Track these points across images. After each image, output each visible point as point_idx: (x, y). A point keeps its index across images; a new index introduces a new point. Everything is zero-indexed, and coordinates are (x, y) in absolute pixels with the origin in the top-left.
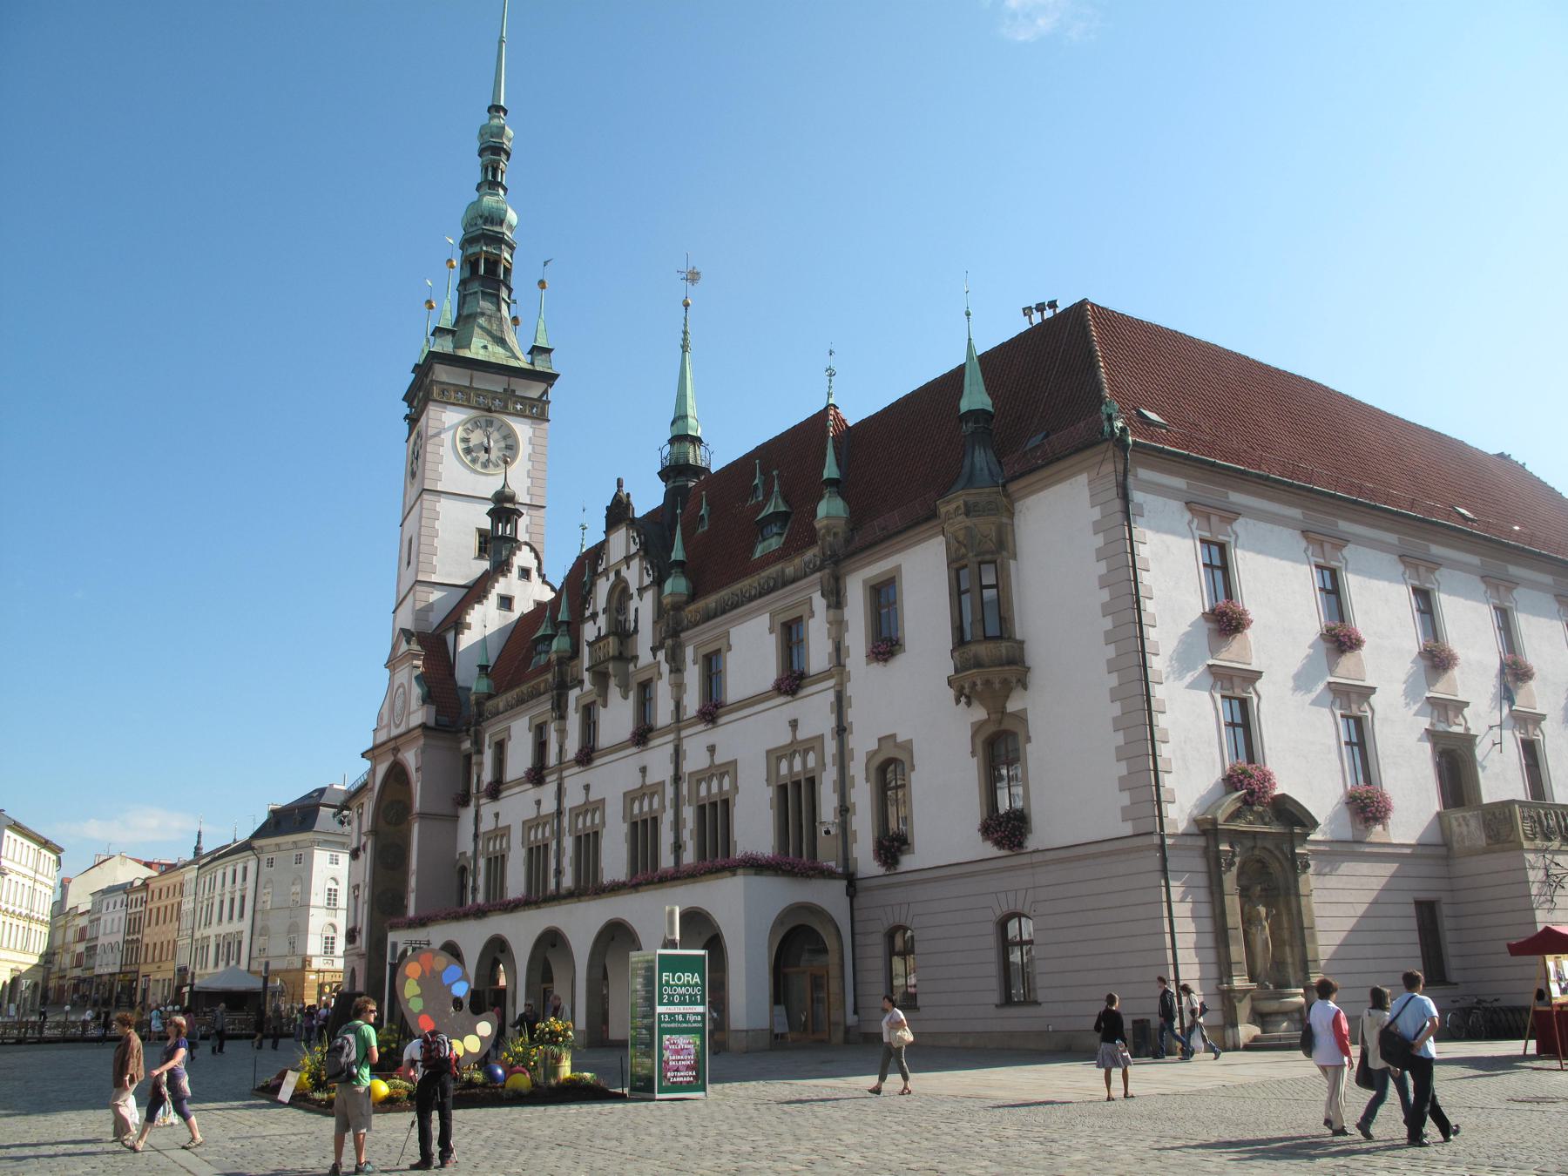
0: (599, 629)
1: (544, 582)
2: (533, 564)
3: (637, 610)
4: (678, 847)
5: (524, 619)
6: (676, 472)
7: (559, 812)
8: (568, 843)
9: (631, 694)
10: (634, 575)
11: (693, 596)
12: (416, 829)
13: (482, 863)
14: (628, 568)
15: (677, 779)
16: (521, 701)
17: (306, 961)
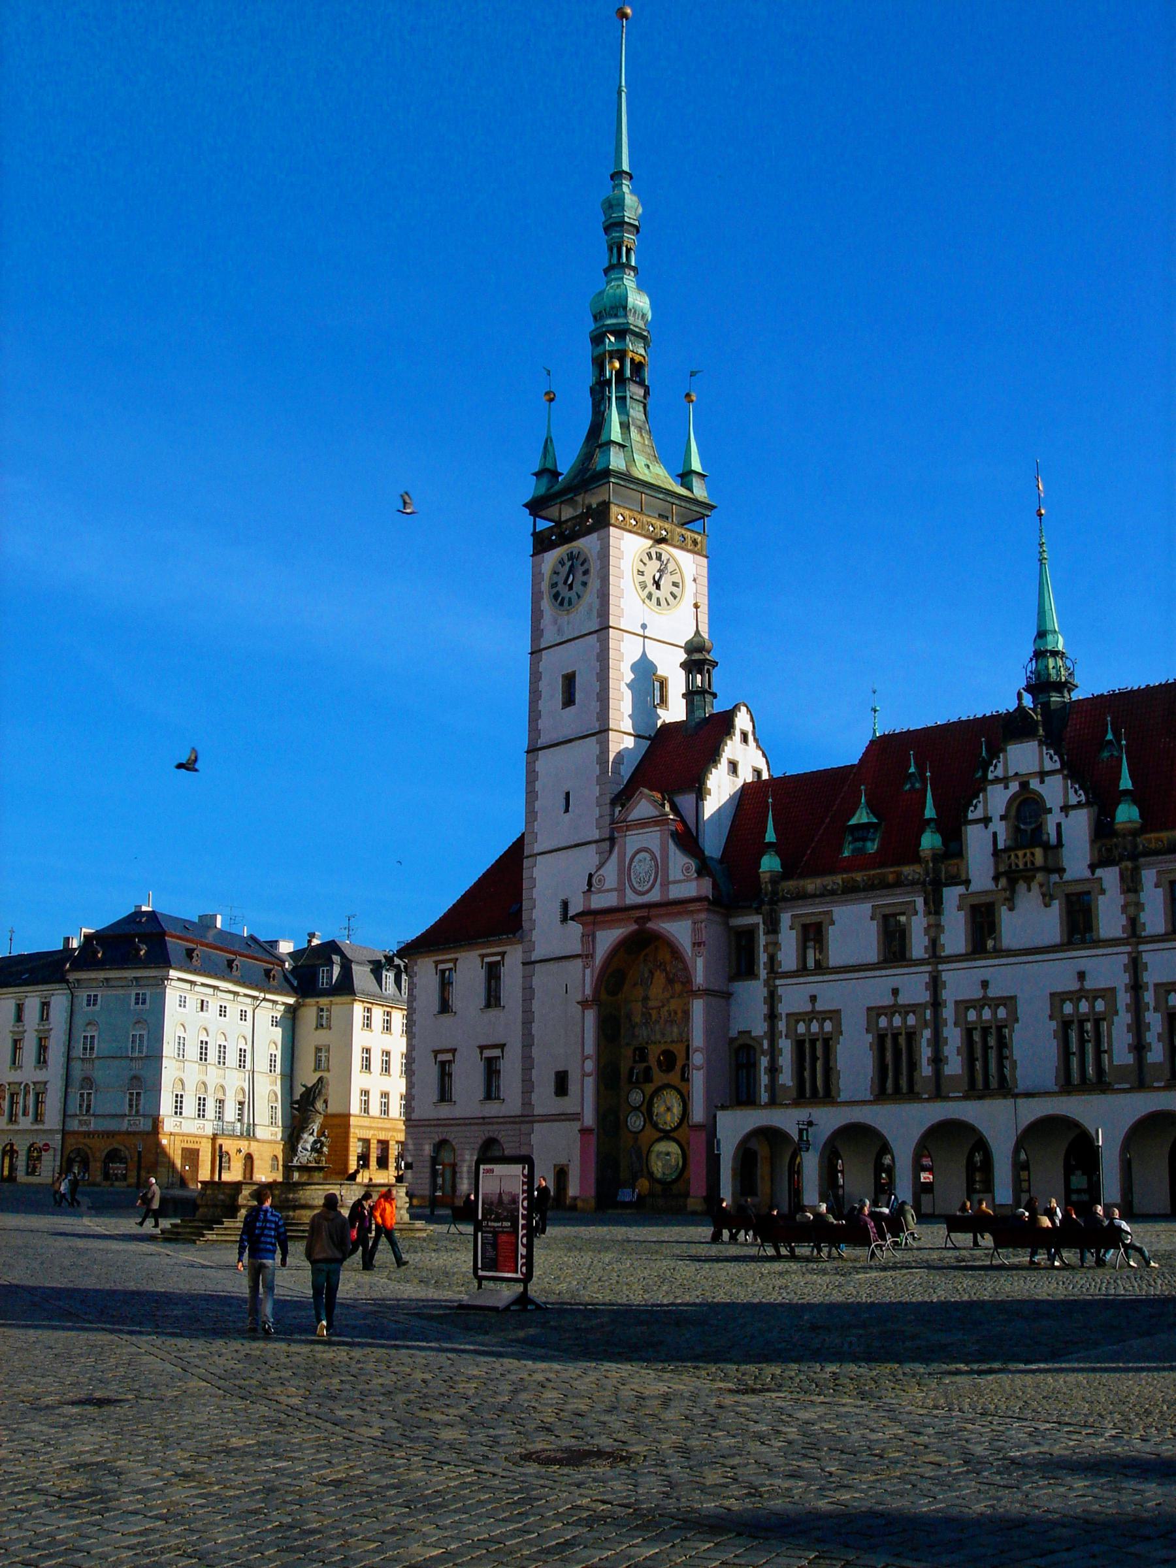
0: (995, 835)
1: (758, 747)
2: (749, 728)
3: (1059, 825)
4: (1139, 1048)
5: (745, 786)
6: (1040, 686)
7: (936, 1004)
8: (953, 1036)
9: (1056, 903)
10: (1053, 791)
11: (1145, 828)
12: (698, 1007)
13: (786, 1046)
14: (1042, 782)
15: (1136, 987)
16: (850, 891)
17: (156, 1122)
